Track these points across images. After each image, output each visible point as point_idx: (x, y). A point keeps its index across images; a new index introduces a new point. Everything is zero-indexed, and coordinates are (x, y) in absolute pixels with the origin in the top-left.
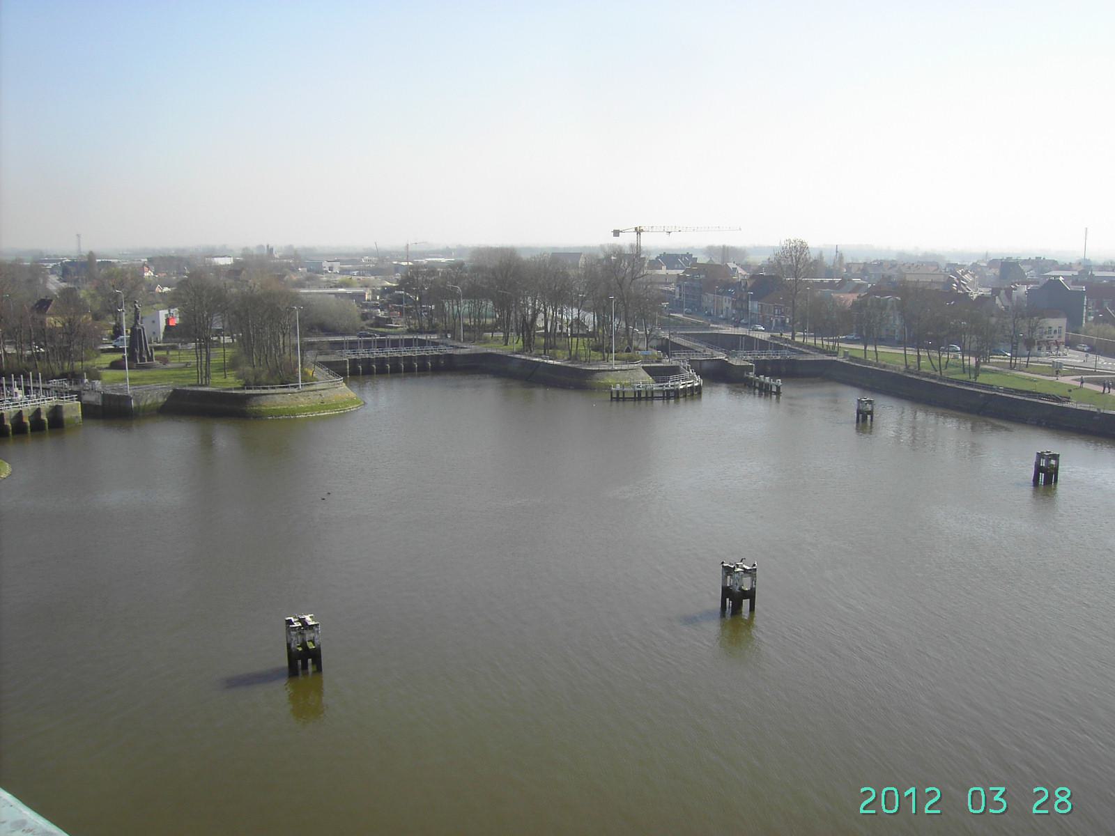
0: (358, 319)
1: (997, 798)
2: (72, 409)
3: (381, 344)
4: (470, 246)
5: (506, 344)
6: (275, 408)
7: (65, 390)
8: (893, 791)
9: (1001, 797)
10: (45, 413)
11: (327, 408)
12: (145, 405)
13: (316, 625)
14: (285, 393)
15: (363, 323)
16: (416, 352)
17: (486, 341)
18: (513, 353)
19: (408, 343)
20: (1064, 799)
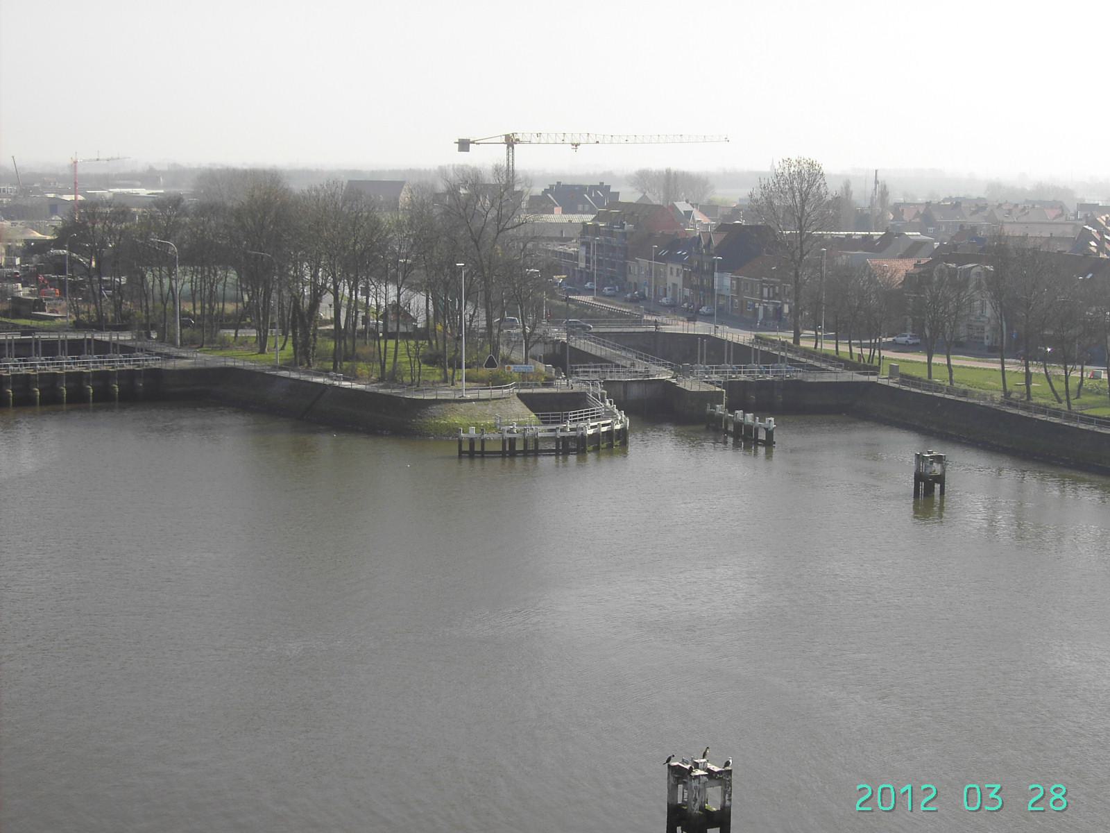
1: (992, 795)
5: (262, 351)
8: (889, 788)
9: (997, 794)
16: (90, 364)
17: (224, 345)
19: (76, 348)
20: (1059, 796)
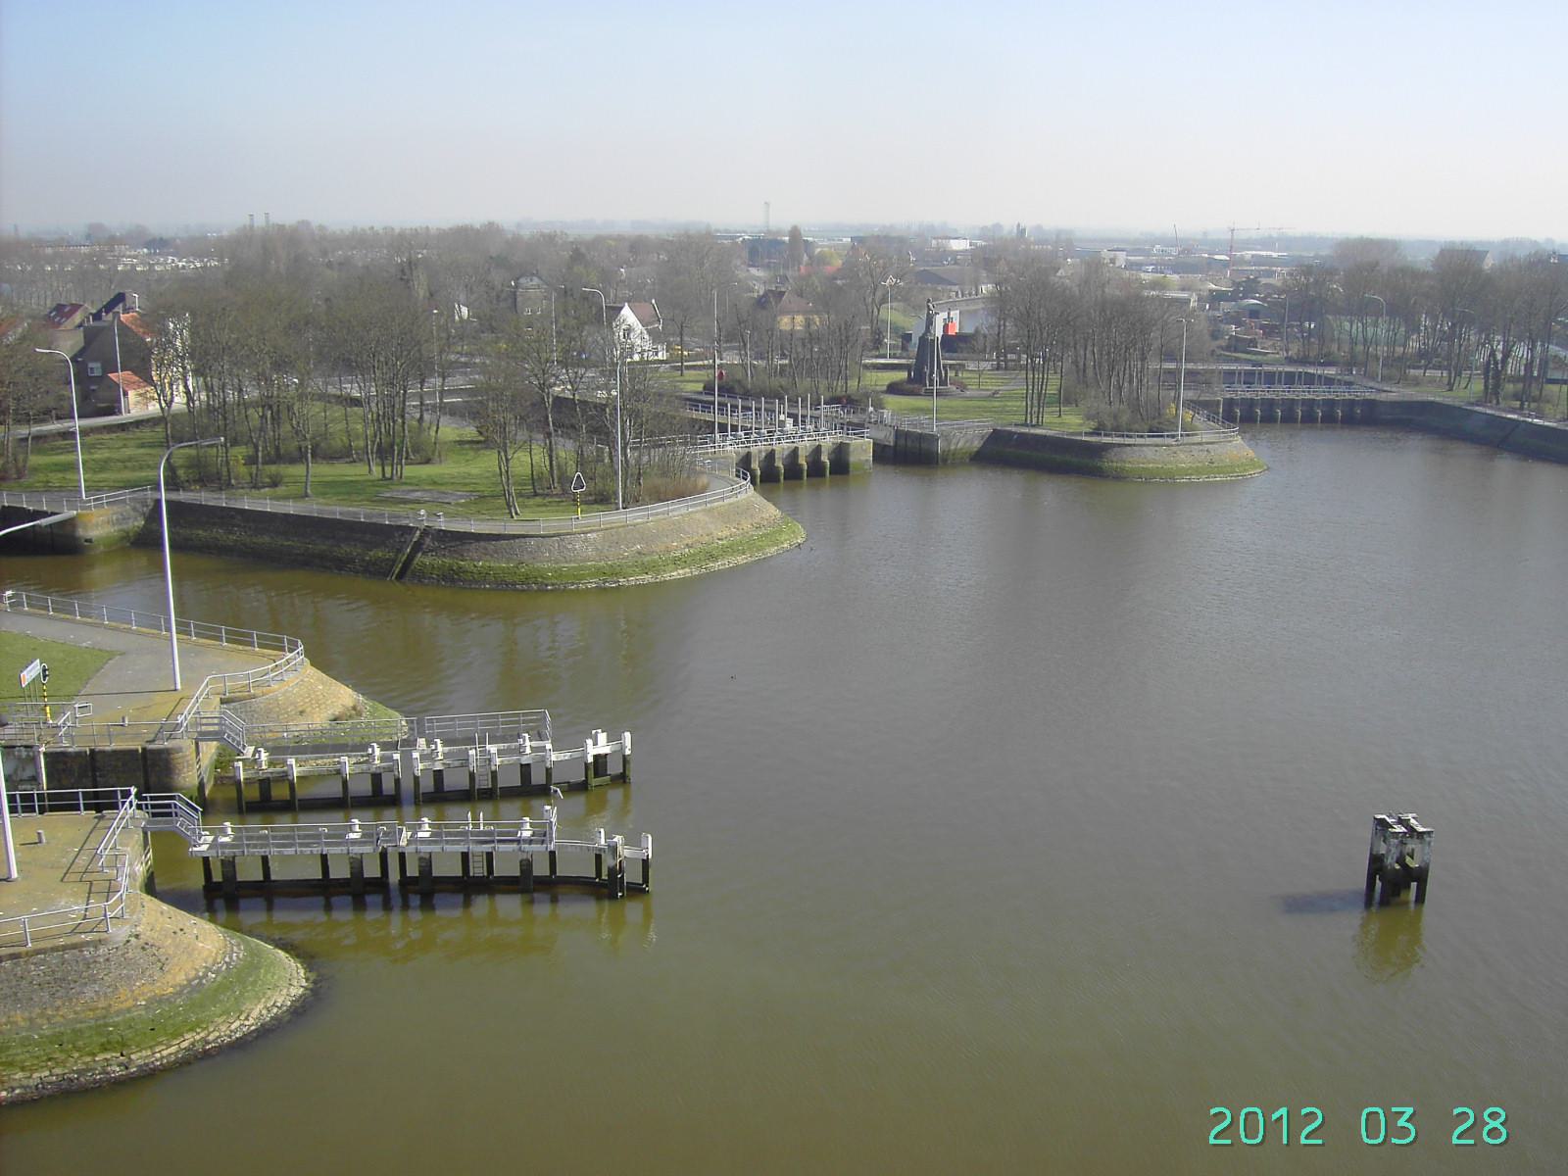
0: (1207, 337)
2: (861, 449)
3: (1249, 378)
4: (1330, 236)
5: (1451, 390)
6: (1144, 466)
7: (841, 421)
10: (826, 454)
11: (1220, 470)
12: (956, 449)
13: (1429, 833)
14: (1157, 446)
16: (1301, 393)
17: (1416, 382)
18: (1472, 404)
19: (1290, 379)
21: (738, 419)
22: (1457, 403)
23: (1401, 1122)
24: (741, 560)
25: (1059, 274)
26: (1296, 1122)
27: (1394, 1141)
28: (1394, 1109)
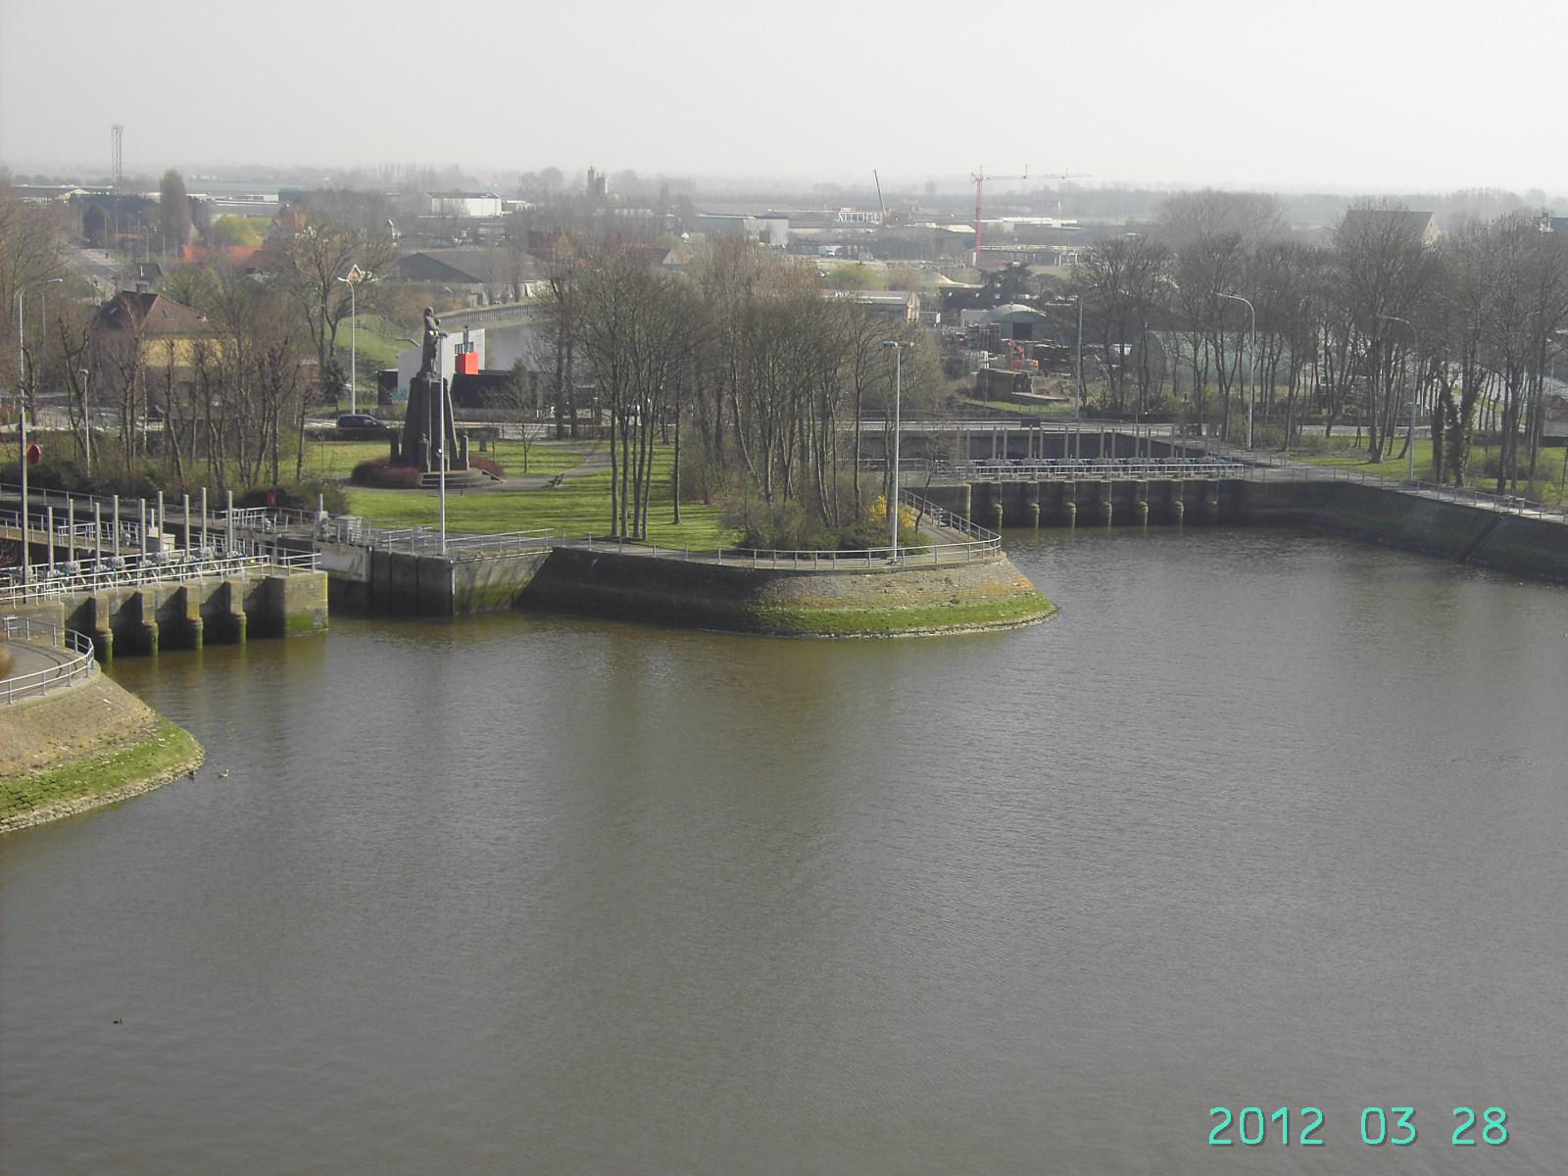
0: (939, 374)
3: (1017, 447)
4: (1153, 189)
5: (1375, 460)
6: (834, 610)
7: (267, 538)
11: (969, 615)
14: (856, 573)
15: (954, 386)
16: (1111, 471)
17: (1314, 448)
18: (1414, 485)
19: (1090, 447)
21: (69, 536)
22: (1386, 485)
23: (1401, 1122)
24: (80, 804)
25: (667, 261)
26: (1295, 1123)
27: (1394, 1141)
28: (1394, 1109)
